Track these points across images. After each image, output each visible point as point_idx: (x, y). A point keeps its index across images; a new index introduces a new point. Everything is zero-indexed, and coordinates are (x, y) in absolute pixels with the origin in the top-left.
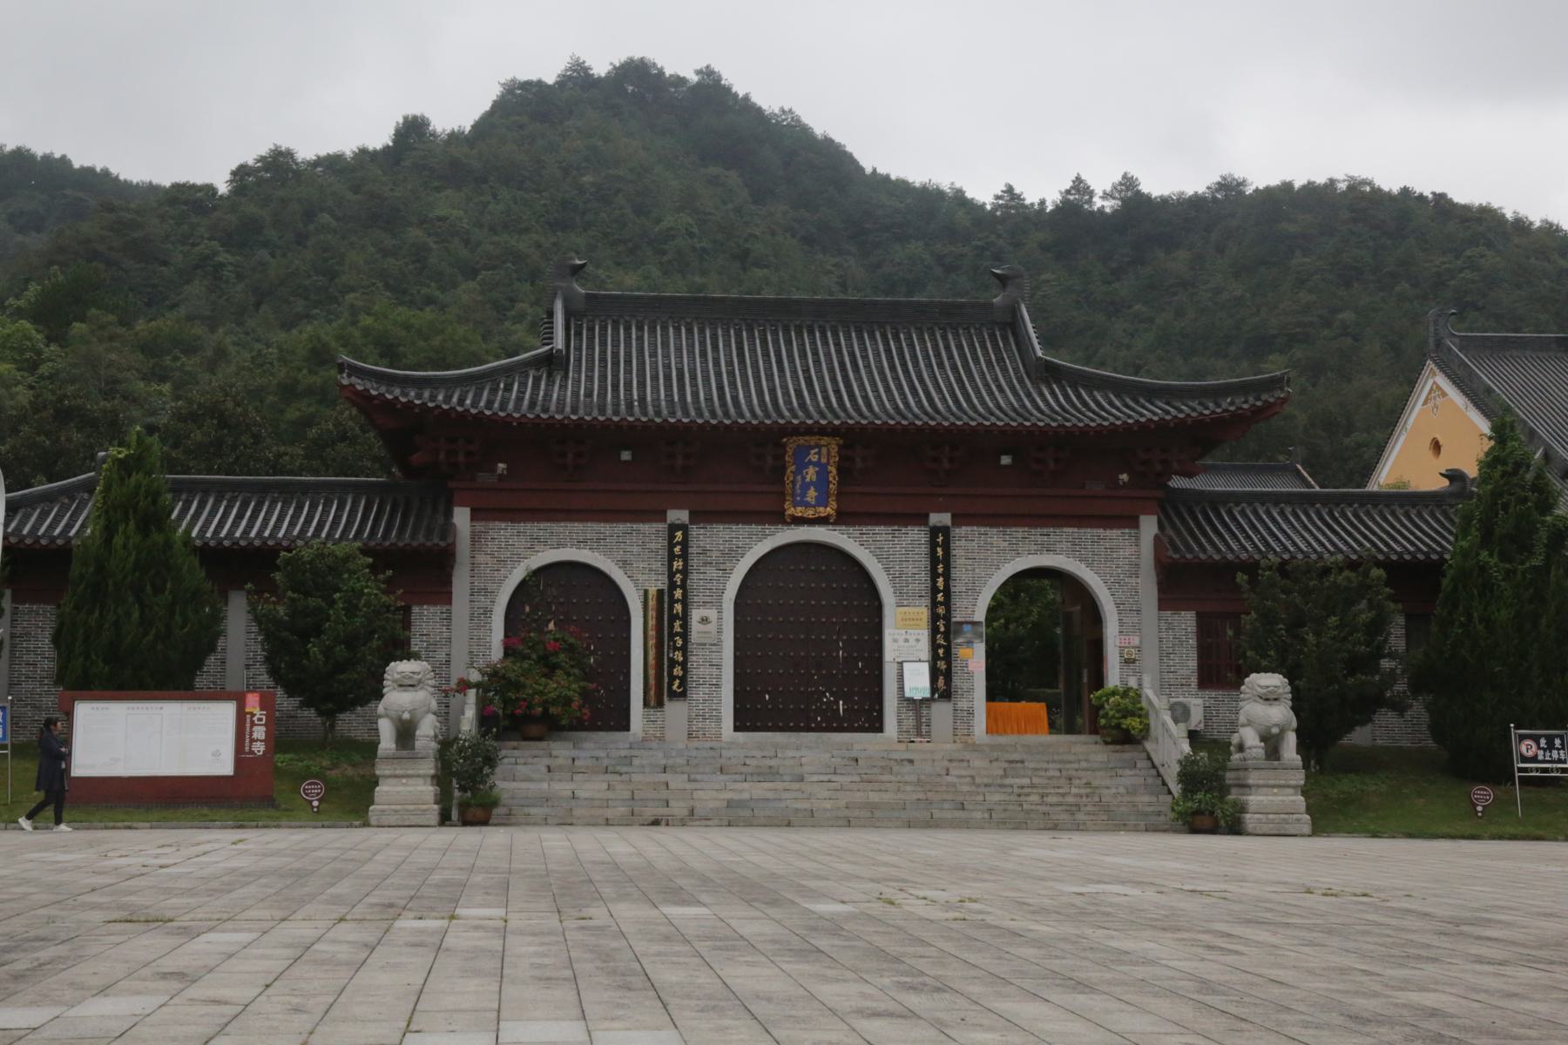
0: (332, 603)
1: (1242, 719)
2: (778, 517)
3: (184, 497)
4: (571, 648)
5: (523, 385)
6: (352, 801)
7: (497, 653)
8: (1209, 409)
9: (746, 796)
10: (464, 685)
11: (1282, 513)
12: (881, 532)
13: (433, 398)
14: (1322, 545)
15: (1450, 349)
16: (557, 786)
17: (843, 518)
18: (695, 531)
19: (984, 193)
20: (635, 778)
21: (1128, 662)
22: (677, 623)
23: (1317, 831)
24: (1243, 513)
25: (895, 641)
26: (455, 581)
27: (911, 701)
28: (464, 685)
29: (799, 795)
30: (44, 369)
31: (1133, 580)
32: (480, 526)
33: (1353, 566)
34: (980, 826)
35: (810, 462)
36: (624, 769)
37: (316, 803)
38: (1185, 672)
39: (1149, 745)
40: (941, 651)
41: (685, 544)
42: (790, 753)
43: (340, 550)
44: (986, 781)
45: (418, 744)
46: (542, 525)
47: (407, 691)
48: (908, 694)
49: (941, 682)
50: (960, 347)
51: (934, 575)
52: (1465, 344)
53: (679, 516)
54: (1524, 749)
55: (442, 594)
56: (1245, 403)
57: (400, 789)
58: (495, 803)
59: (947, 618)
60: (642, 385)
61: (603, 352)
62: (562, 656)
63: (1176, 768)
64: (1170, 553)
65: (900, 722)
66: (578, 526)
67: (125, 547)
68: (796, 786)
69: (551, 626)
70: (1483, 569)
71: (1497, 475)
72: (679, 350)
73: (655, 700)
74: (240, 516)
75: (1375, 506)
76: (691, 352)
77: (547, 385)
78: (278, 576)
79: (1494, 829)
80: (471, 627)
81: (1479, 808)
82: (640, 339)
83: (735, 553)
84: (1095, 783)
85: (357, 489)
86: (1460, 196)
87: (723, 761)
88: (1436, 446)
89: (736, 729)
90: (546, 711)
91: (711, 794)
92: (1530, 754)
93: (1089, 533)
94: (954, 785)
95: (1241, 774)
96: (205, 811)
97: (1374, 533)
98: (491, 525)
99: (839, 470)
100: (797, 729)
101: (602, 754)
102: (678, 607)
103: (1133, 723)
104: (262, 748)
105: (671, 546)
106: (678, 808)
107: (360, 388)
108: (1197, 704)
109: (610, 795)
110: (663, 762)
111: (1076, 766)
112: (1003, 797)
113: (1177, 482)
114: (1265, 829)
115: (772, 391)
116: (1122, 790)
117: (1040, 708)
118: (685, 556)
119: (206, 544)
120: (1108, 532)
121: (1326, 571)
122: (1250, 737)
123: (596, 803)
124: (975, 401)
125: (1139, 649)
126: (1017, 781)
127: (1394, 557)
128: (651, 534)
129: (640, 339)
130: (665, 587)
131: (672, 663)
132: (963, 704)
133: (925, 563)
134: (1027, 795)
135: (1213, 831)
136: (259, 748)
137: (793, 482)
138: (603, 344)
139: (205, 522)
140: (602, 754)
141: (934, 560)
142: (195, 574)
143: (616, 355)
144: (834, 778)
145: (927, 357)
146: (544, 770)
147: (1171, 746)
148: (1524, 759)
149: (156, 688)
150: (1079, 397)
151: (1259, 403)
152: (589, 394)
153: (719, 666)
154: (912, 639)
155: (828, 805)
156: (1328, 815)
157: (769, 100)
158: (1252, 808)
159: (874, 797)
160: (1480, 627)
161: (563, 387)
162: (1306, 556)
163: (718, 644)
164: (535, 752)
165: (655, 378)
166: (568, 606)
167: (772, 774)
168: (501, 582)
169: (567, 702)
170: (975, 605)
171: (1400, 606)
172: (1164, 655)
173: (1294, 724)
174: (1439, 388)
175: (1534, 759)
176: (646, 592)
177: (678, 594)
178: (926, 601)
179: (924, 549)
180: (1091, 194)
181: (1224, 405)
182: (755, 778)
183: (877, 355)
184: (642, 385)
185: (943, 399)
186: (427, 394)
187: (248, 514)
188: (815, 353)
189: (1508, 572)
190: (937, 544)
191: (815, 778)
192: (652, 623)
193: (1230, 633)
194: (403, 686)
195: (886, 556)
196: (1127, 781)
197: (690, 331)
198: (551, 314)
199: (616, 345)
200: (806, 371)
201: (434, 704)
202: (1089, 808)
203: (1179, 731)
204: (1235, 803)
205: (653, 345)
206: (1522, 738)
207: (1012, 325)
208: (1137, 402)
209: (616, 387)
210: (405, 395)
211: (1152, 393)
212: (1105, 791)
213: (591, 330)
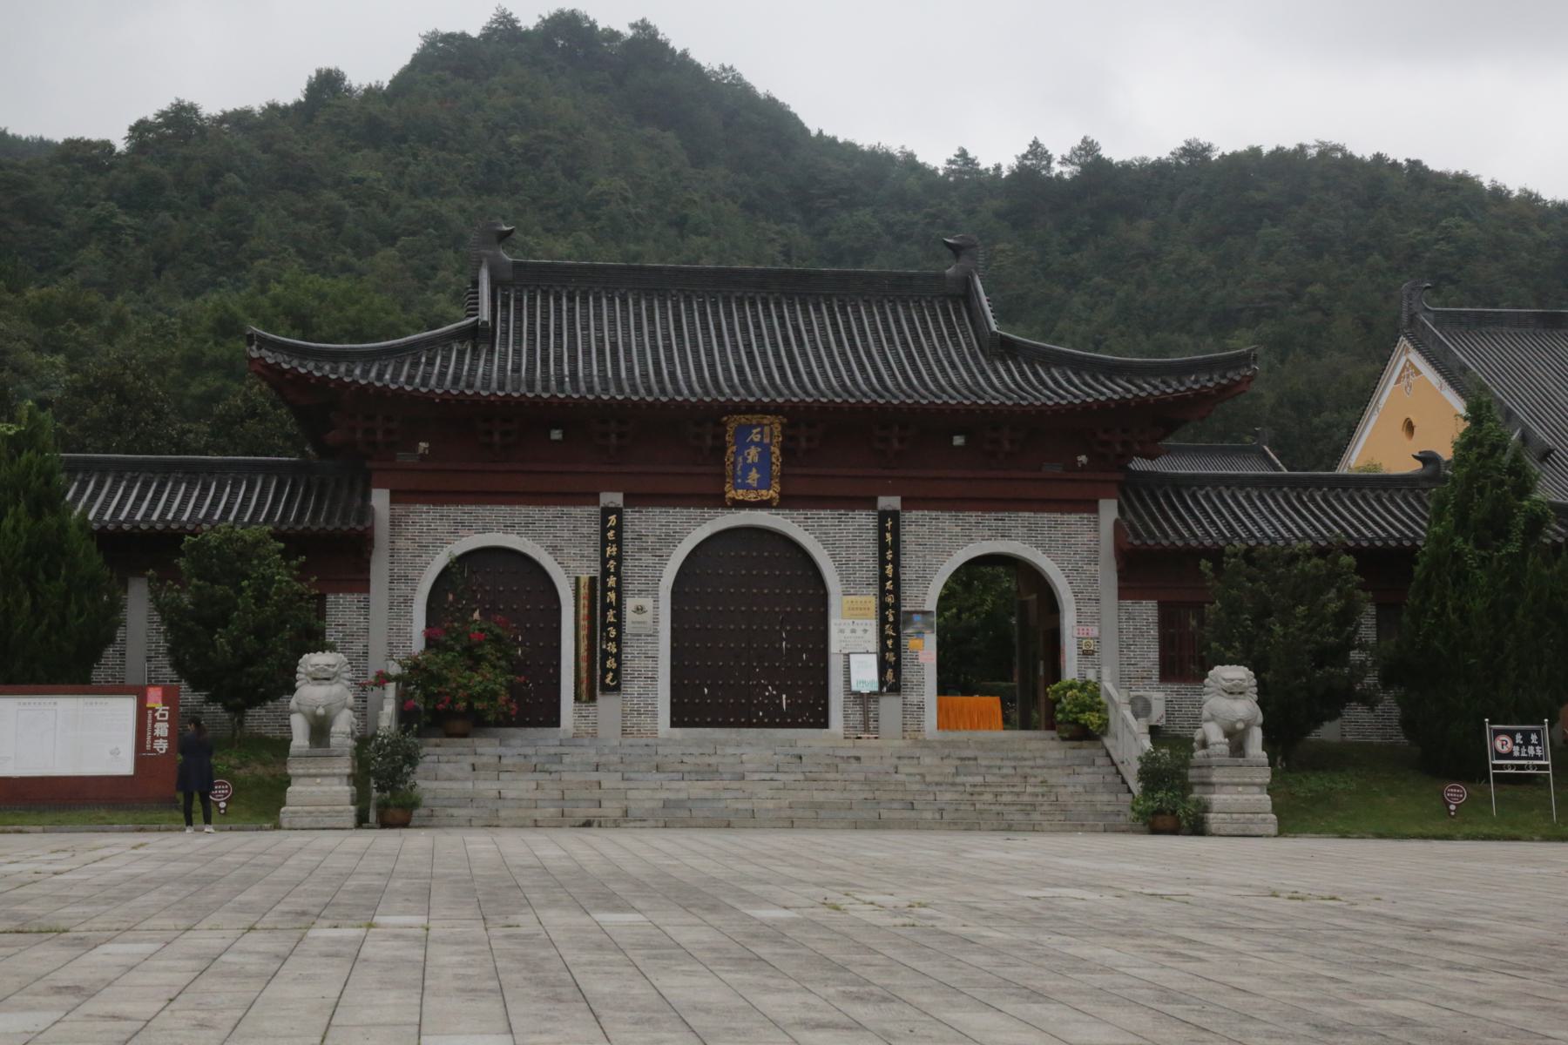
0: (241, 590)
1: (1206, 714)
2: (719, 501)
3: (80, 476)
4: (498, 640)
5: (446, 359)
6: (264, 803)
7: (418, 644)
8: (1174, 387)
9: (683, 795)
11: (1248, 498)
13: (349, 372)
14: (1289, 530)
15: (1424, 325)
17: (787, 501)
18: (629, 515)
19: (936, 157)
20: (566, 776)
21: (1086, 653)
22: (611, 613)
23: (1281, 833)
24: (1207, 498)
25: (842, 631)
26: (373, 568)
27: (859, 695)
28: (383, 679)
31: (1092, 568)
33: (1322, 552)
34: (929, 828)
35: (752, 442)
36: (555, 767)
37: (223, 805)
38: (1147, 664)
39: (1108, 742)
40: (890, 642)
41: (619, 528)
42: (730, 751)
44: (937, 779)
45: (332, 741)
46: (467, 508)
47: (321, 686)
48: (855, 688)
49: (890, 675)
50: (910, 321)
51: (883, 562)
52: (1441, 320)
53: (613, 498)
54: (1498, 744)
55: (358, 581)
56: (1209, 381)
57: (314, 789)
58: (415, 804)
59: (897, 606)
60: (573, 359)
61: (532, 324)
62: (488, 648)
63: (1137, 766)
64: (1131, 538)
65: (846, 717)
66: (504, 509)
67: (14, 530)
68: (736, 785)
69: (476, 615)
70: (1457, 556)
71: (1472, 456)
72: (612, 322)
73: (586, 695)
74: (140, 498)
75: (1345, 490)
76: (626, 325)
77: (472, 359)
78: (182, 563)
79: (1467, 829)
80: (390, 617)
81: (1453, 807)
82: (571, 310)
83: (671, 539)
84: (1052, 781)
85: (268, 469)
86: (1435, 164)
87: (658, 759)
88: (1409, 427)
89: (673, 725)
90: (470, 705)
91: (646, 793)
92: (1505, 750)
93: (1044, 518)
94: (903, 784)
95: (1205, 771)
96: (103, 813)
97: (1344, 518)
98: (412, 508)
99: (784, 451)
101: (530, 751)
102: (612, 596)
103: (1091, 718)
104: (165, 746)
105: (604, 530)
106: (611, 809)
107: (270, 361)
108: (1158, 698)
109: (539, 795)
110: (596, 759)
111: (1031, 763)
112: (956, 796)
113: (1139, 464)
114: (1229, 829)
115: (712, 366)
116: (1080, 789)
117: (993, 703)
118: (619, 541)
119: (104, 527)
120: (1066, 517)
121: (1294, 558)
122: (1214, 732)
124: (927, 378)
125: (1098, 640)
126: (970, 779)
127: (1365, 544)
128: (583, 518)
129: (571, 310)
130: (598, 575)
131: (606, 655)
132: (913, 698)
133: (873, 548)
134: (981, 794)
135: (1175, 831)
136: (162, 746)
137: (734, 464)
138: (532, 316)
139: (101, 504)
140: (530, 751)
141: (883, 547)
143: (545, 327)
144: (776, 776)
145: (875, 331)
147: (1131, 742)
148: (1500, 756)
149: (49, 682)
150: (1036, 374)
151: (1224, 382)
152: (517, 369)
153: (655, 658)
154: (859, 630)
156: (1295, 814)
157: (708, 56)
158: (1215, 807)
159: (819, 797)
161: (489, 361)
162: (1273, 542)
163: (654, 634)
164: (459, 749)
165: (587, 352)
166: (493, 592)
167: (708, 773)
168: (422, 569)
170: (925, 594)
171: (1370, 594)
172: (1124, 646)
173: (1260, 719)
174: (1412, 365)
175: (1509, 756)
176: (577, 579)
177: (612, 581)
179: (872, 535)
180: (1049, 159)
181: (1188, 384)
182: (694, 776)
183: (823, 328)
184: (573, 359)
185: (893, 376)
186: (342, 369)
187: (150, 495)
188: (757, 326)
189: (1483, 559)
190: (886, 530)
191: (756, 777)
192: (584, 612)
193: (1193, 623)
195: (833, 542)
196: (1084, 779)
197: (624, 302)
198: (476, 284)
199: (545, 318)
200: (748, 346)
201: (350, 699)
202: (1045, 808)
203: (1139, 727)
204: (1198, 802)
205: (585, 317)
206: (1497, 733)
207: (965, 296)
208: (1097, 380)
209: (545, 361)
210: (319, 368)
211: (1113, 370)
212: (1061, 790)
213: (519, 301)
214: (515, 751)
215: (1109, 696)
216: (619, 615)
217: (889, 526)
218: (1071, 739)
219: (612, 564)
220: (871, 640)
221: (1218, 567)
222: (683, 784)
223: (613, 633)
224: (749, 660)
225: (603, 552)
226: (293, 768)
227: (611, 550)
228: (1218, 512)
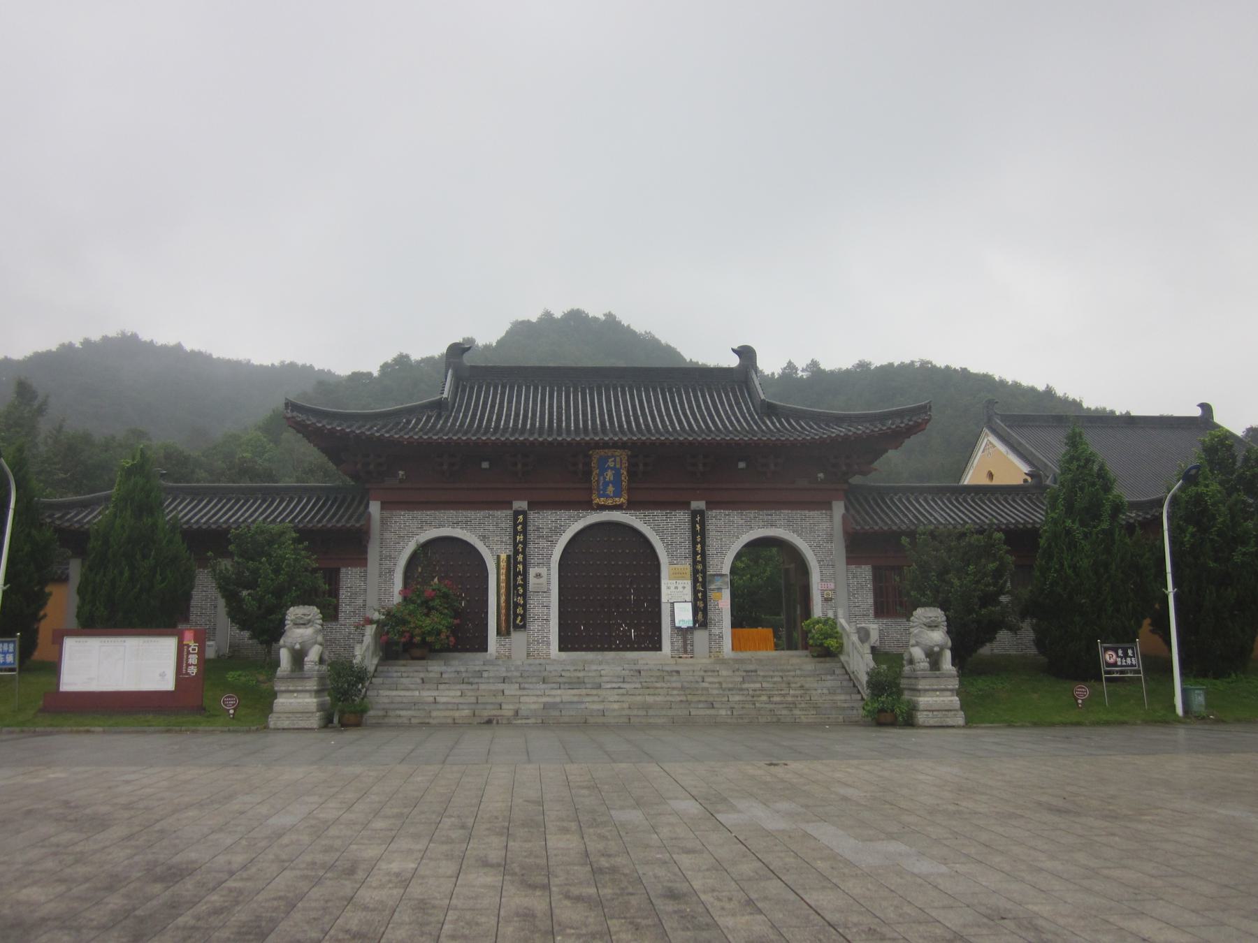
1: (912, 642)
2: (588, 506)
4: (445, 596)
5: (419, 420)
7: (397, 599)
8: (878, 427)
9: (558, 699)
10: (370, 622)
16: (425, 693)
17: (632, 505)
20: (482, 687)
21: (827, 600)
23: (969, 723)
24: (900, 500)
26: (370, 550)
27: (680, 629)
28: (370, 622)
29: (596, 699)
30: (266, 456)
31: (829, 545)
32: (387, 513)
33: (981, 532)
35: (609, 468)
39: (843, 658)
41: (525, 524)
42: (594, 667)
43: (275, 528)
44: (730, 686)
45: (306, 667)
47: (302, 628)
49: (700, 615)
51: (694, 543)
53: (521, 505)
55: (360, 559)
59: (704, 572)
60: (499, 419)
62: (437, 602)
63: (864, 679)
67: (123, 526)
68: (594, 692)
70: (1068, 532)
75: (985, 494)
78: (232, 548)
80: (379, 584)
82: (503, 394)
83: (559, 530)
84: (807, 686)
87: (545, 674)
90: (423, 640)
92: (1112, 661)
93: (798, 514)
94: (707, 689)
95: (913, 681)
96: (150, 717)
100: (602, 649)
102: (520, 567)
103: (831, 642)
105: (515, 525)
106: (508, 710)
108: (874, 627)
109: (461, 700)
113: (856, 480)
114: (932, 722)
116: (825, 691)
117: (768, 632)
118: (525, 532)
120: (812, 513)
121: (963, 535)
122: (918, 653)
123: (450, 707)
125: (834, 591)
126: (752, 685)
128: (503, 518)
131: (516, 605)
132: (715, 631)
133: (688, 534)
134: (759, 696)
135: (893, 724)
136: (193, 671)
137: (598, 481)
141: (694, 533)
144: (622, 685)
146: (419, 681)
148: (1108, 665)
150: (790, 424)
154: (680, 587)
155: (616, 706)
156: (976, 709)
157: (639, 327)
158: (921, 707)
159: (650, 699)
160: (1069, 572)
166: (447, 567)
167: (577, 683)
169: (439, 633)
170: (723, 562)
173: (950, 644)
175: (1115, 664)
176: (498, 557)
177: (520, 558)
179: (687, 526)
180: (797, 369)
191: (609, 686)
192: (503, 577)
193: (898, 579)
194: (297, 625)
195: (662, 532)
196: (828, 684)
200: (610, 411)
201: (320, 638)
204: (909, 702)
206: (1106, 649)
213: (472, 388)
214: (453, 669)
215: (843, 628)
216: (525, 580)
218: (818, 656)
220: (688, 593)
222: (559, 692)
223: (521, 591)
224: (609, 605)
225: (515, 539)
227: (520, 538)
228: (907, 508)
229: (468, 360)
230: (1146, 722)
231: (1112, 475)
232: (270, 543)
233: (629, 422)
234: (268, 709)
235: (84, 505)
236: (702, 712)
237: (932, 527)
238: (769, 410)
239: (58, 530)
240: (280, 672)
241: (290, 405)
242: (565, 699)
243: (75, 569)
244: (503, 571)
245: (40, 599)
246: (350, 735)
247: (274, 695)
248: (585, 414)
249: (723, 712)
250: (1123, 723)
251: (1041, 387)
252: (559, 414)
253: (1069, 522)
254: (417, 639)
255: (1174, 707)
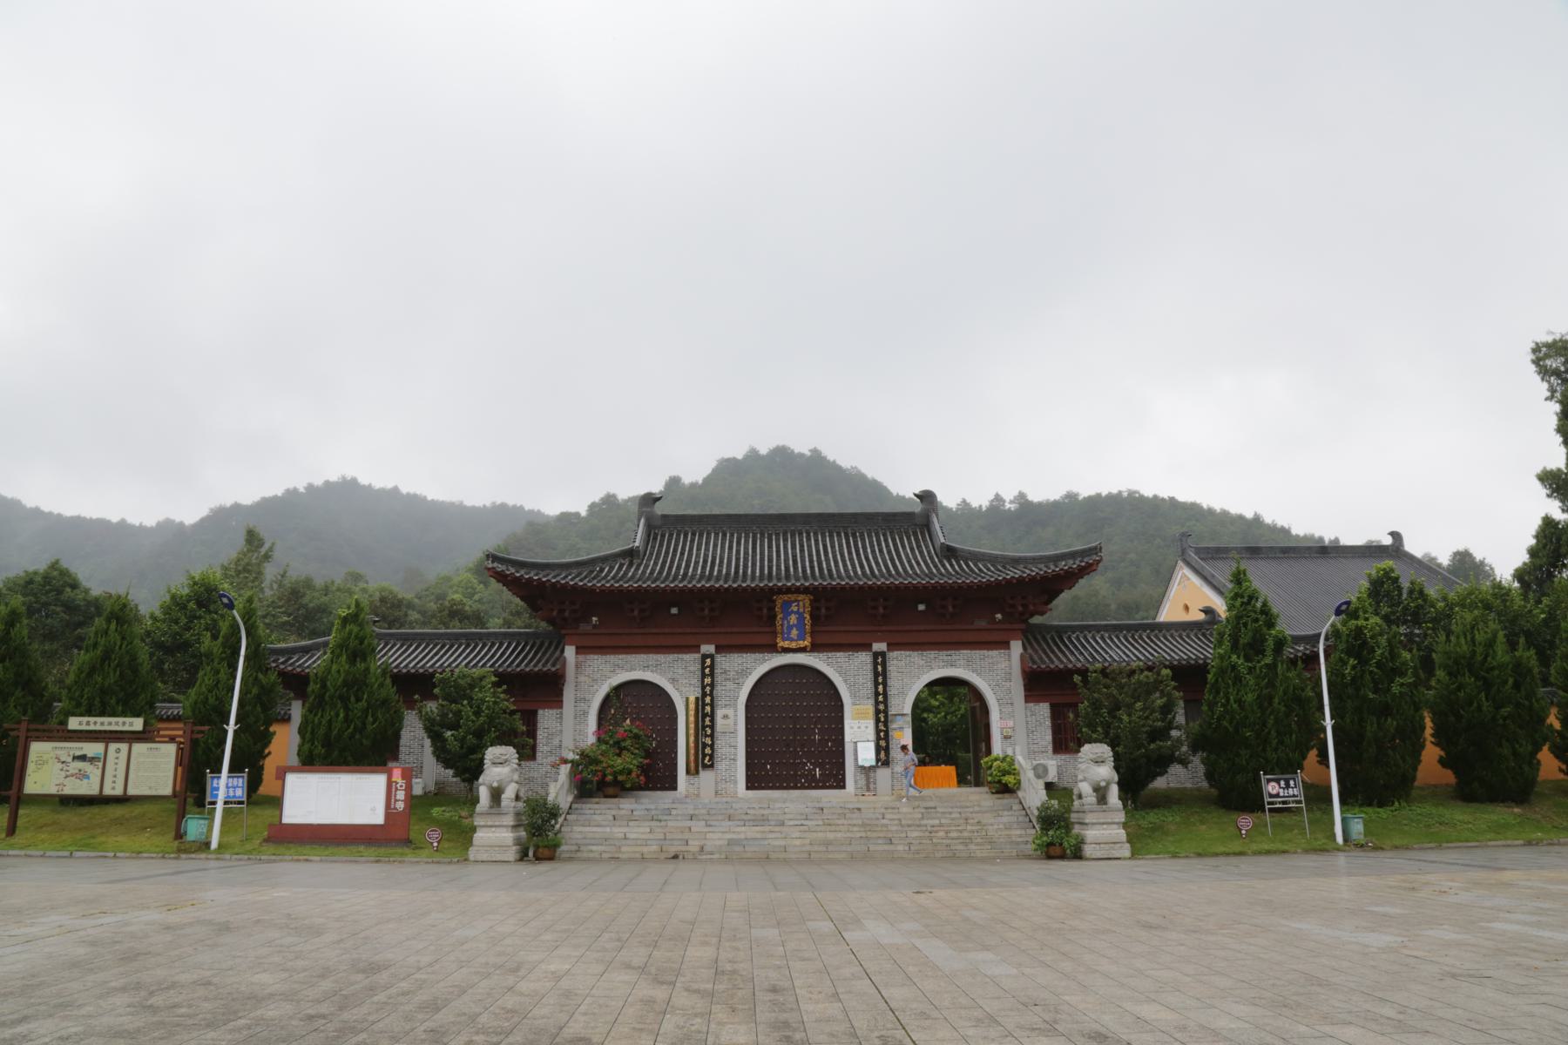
2: (773, 648)
4: (636, 737)
7: (591, 739)
10: (565, 761)
11: (1102, 638)
12: (841, 657)
16: (616, 830)
17: (815, 648)
18: (719, 658)
23: (1135, 854)
24: (1078, 639)
27: (863, 768)
28: (565, 761)
30: (476, 597)
32: (581, 657)
33: (1150, 669)
39: (1020, 794)
41: (712, 667)
42: (778, 805)
43: (477, 672)
47: (500, 766)
51: (876, 684)
53: (708, 648)
56: (1074, 564)
58: (556, 846)
59: (886, 712)
60: (688, 566)
62: (628, 742)
63: (1036, 813)
70: (1234, 667)
78: (436, 691)
79: (1254, 847)
80: (572, 726)
82: (692, 541)
83: (745, 672)
89: (748, 788)
96: (362, 848)
99: (812, 616)
100: (788, 788)
102: (708, 709)
103: (1009, 779)
105: (703, 668)
106: (694, 846)
108: (1053, 764)
113: (1036, 620)
114: (1099, 855)
118: (712, 675)
121: (1133, 672)
122: (1085, 788)
128: (689, 663)
129: (692, 541)
131: (705, 746)
133: (870, 676)
135: (1062, 857)
136: (400, 806)
141: (876, 674)
142: (390, 691)
147: (1034, 796)
148: (1271, 796)
155: (798, 842)
156: (1140, 842)
157: (845, 462)
158: (1088, 840)
159: (831, 836)
163: (734, 732)
166: (636, 706)
167: (762, 820)
169: (630, 772)
172: (1030, 732)
175: (1277, 795)
177: (708, 700)
178: (872, 701)
179: (870, 667)
188: (802, 546)
192: (692, 719)
195: (846, 672)
196: (1005, 819)
200: (794, 556)
201: (516, 777)
203: (1040, 785)
206: (1269, 781)
213: (663, 536)
216: (712, 721)
217: (880, 662)
219: (708, 689)
221: (1085, 681)
224: (795, 745)
226: (478, 821)
227: (708, 680)
229: (660, 509)
230: (1306, 851)
231: (1275, 610)
232: (472, 687)
233: (812, 568)
234: (469, 842)
235: (305, 650)
236: (880, 848)
237: (1099, 666)
238: (949, 552)
239: (282, 674)
240: (479, 808)
241: (492, 557)
242: (750, 835)
243: (297, 710)
244: (692, 713)
245: (266, 738)
246: (544, 867)
247: (474, 829)
248: (770, 560)
249: (900, 848)
250: (1284, 852)
251: (1249, 515)
252: (746, 559)
253: (1234, 657)
254: (610, 778)
255: (1334, 835)
